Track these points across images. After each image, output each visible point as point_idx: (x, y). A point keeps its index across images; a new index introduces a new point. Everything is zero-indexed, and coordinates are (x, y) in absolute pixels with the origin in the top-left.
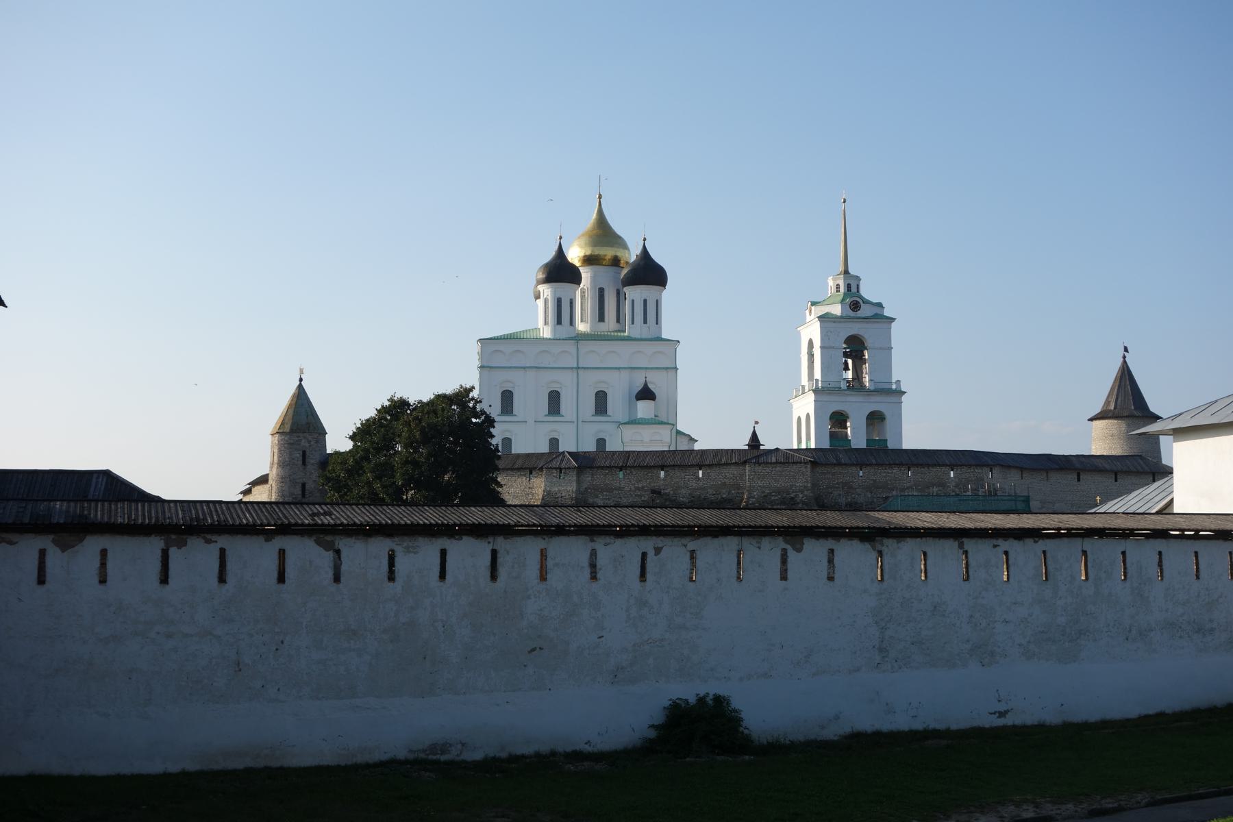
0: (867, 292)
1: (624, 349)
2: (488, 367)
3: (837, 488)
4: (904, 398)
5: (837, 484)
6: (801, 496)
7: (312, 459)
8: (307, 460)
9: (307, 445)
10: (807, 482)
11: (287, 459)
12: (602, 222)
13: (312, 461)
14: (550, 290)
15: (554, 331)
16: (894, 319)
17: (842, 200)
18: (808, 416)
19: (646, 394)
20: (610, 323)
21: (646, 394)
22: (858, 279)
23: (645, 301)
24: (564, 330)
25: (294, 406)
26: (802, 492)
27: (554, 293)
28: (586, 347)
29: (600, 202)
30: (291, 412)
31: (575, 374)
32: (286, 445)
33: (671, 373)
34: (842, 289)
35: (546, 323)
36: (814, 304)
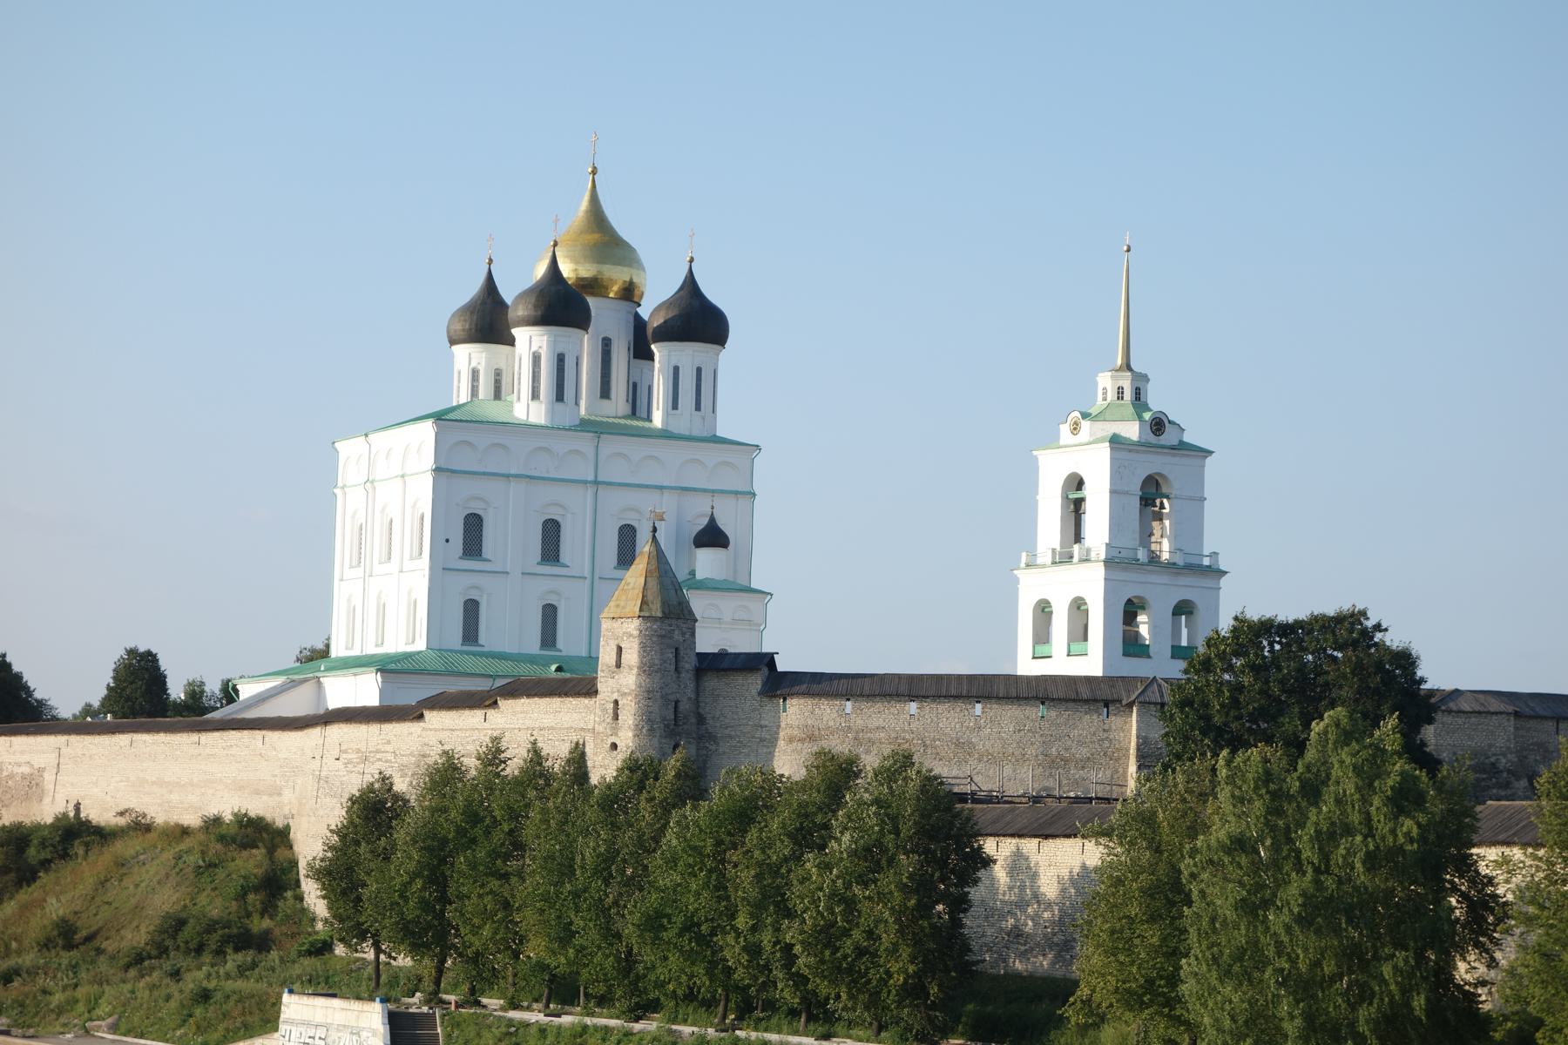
0: (1157, 401)
1: (673, 454)
2: (448, 470)
3: (1533, 750)
4: (1224, 581)
5: (1532, 744)
6: (1504, 761)
7: (687, 662)
8: (681, 664)
9: (681, 639)
10: (1509, 740)
11: (657, 662)
12: (597, 218)
13: (687, 666)
14: (545, 338)
15: (551, 413)
16: (1211, 453)
17: (1125, 248)
18: (1078, 606)
19: (712, 536)
20: (618, 403)
21: (712, 536)
22: (1145, 378)
23: (699, 370)
24: (566, 416)
25: (656, 574)
26: (1504, 755)
27: (553, 343)
28: (611, 445)
29: (594, 181)
30: (653, 583)
31: (590, 492)
32: (654, 639)
33: (743, 502)
34: (1128, 395)
35: (535, 395)
36: (1085, 416)
